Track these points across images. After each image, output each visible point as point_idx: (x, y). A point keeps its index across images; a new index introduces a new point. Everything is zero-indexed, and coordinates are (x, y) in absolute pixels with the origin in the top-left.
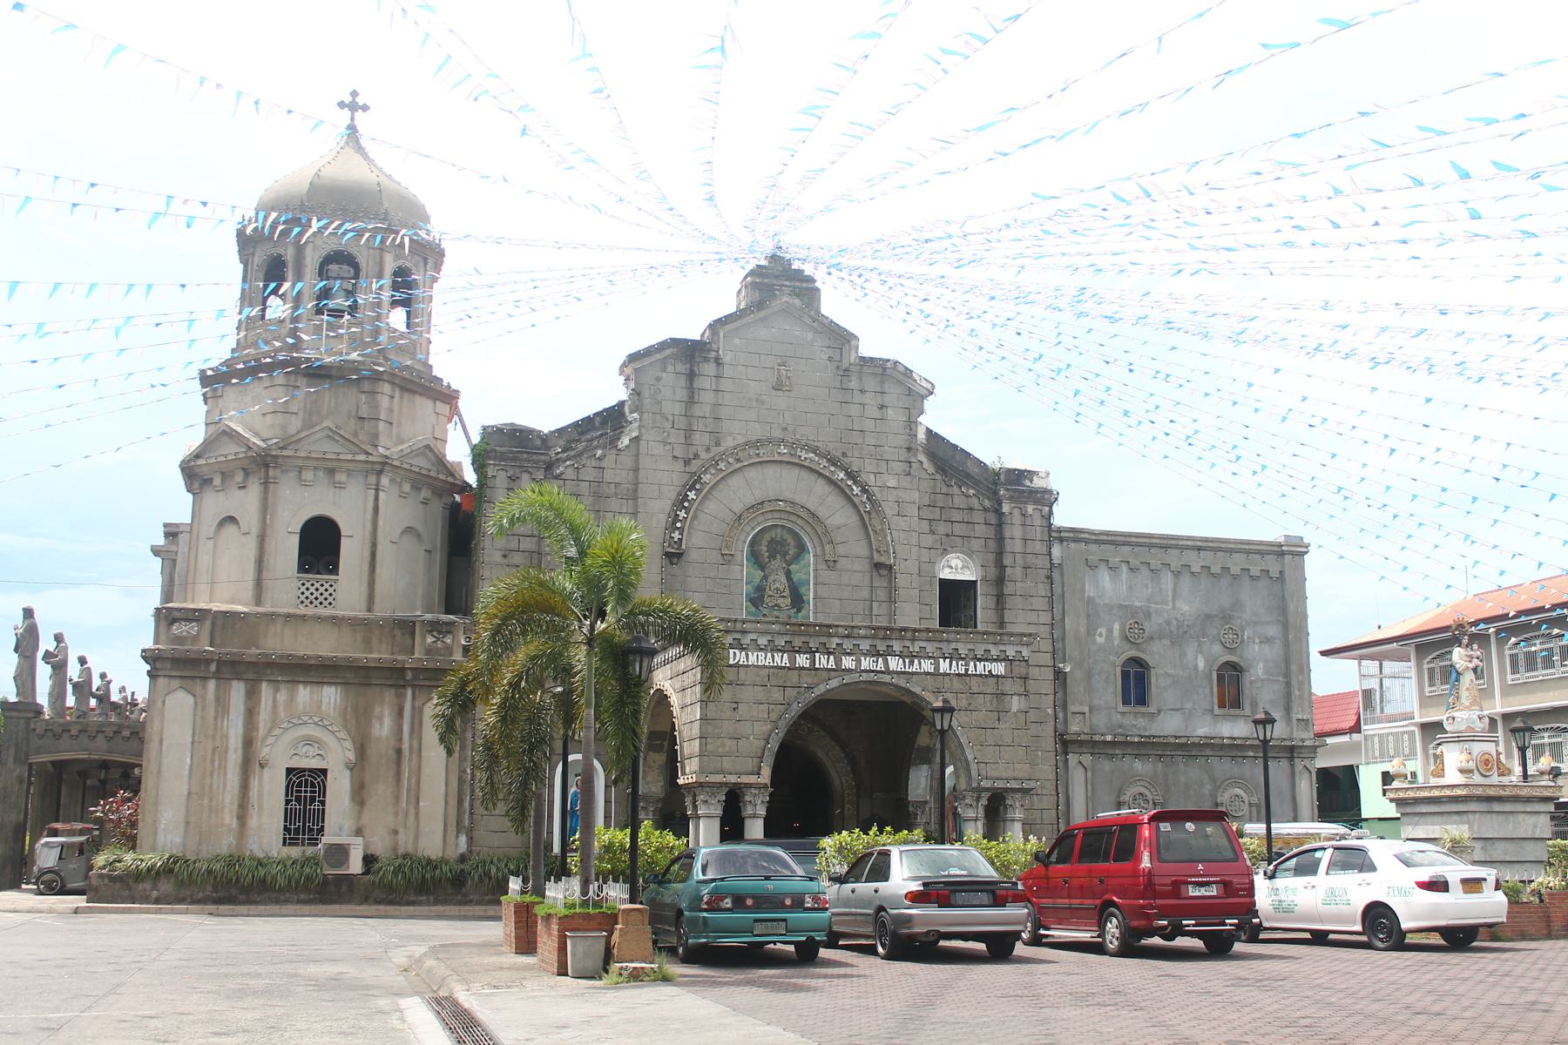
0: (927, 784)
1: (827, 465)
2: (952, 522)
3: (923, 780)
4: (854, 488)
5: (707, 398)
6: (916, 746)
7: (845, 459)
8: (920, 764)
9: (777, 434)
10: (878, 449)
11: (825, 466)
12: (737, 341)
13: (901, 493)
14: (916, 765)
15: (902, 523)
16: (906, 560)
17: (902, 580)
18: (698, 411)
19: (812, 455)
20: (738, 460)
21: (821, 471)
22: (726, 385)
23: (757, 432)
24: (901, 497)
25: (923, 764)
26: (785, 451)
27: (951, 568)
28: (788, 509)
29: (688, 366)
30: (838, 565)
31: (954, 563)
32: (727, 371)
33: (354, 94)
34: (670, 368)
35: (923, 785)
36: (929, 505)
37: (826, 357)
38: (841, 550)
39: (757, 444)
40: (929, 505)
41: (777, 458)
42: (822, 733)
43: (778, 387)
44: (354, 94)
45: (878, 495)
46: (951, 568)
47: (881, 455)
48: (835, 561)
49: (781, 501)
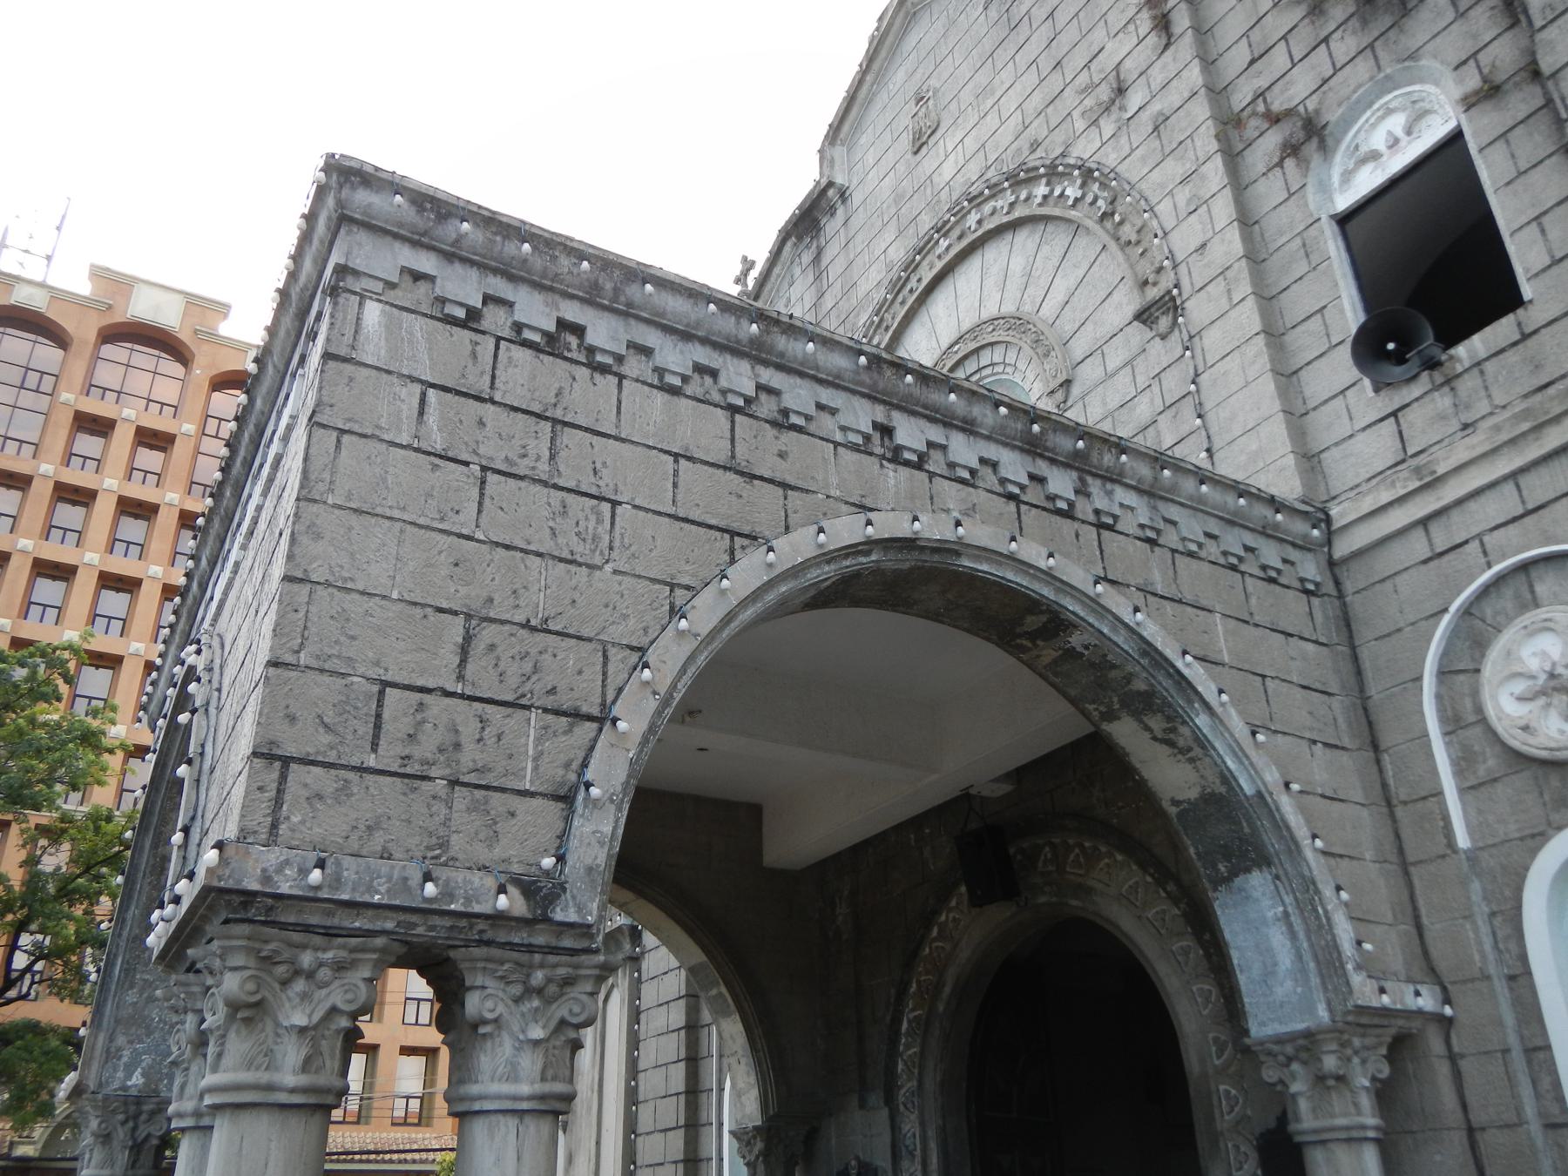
0: (1299, 957)
1: (1013, 198)
2: (1326, 40)
3: (1278, 938)
4: (1068, 192)
5: (835, 271)
6: (1173, 811)
7: (1040, 153)
8: (1234, 874)
9: (927, 222)
10: (1093, 66)
11: (1012, 205)
12: (863, 140)
13: (1156, 107)
14: (1228, 880)
15: (1174, 169)
16: (1203, 246)
17: (1198, 310)
18: (828, 302)
19: (987, 208)
20: (887, 328)
21: (1005, 219)
22: (856, 222)
23: (898, 253)
24: (1160, 113)
25: (1248, 870)
26: (947, 243)
27: (1374, 156)
28: (973, 346)
29: (815, 245)
30: (1076, 390)
31: (1378, 141)
32: (857, 198)
33: (745, 259)
34: (797, 271)
35: (1285, 960)
36: (1252, 62)
37: (981, 9)
38: (1079, 348)
39: (911, 267)
40: (1252, 62)
41: (939, 265)
42: (1119, 857)
43: (919, 144)
44: (745, 259)
45: (1110, 158)
46: (1374, 156)
47: (1101, 71)
48: (1067, 383)
49: (956, 343)
